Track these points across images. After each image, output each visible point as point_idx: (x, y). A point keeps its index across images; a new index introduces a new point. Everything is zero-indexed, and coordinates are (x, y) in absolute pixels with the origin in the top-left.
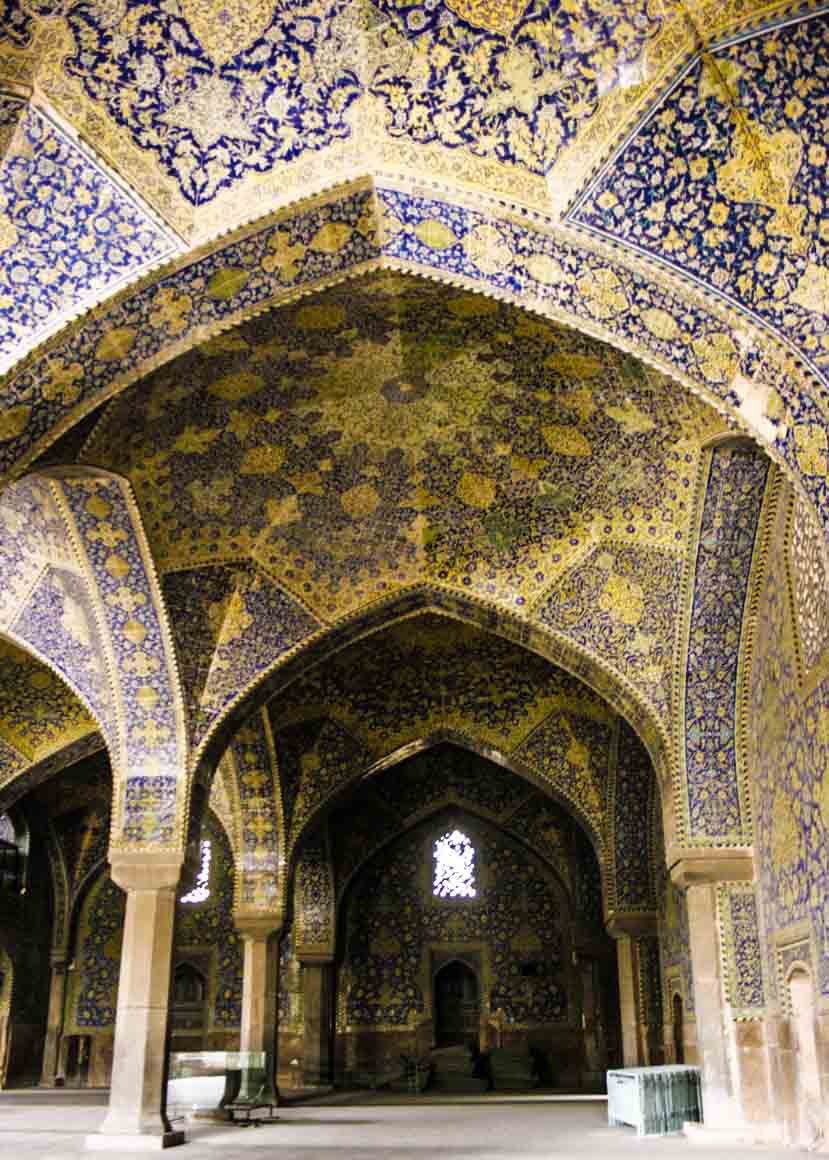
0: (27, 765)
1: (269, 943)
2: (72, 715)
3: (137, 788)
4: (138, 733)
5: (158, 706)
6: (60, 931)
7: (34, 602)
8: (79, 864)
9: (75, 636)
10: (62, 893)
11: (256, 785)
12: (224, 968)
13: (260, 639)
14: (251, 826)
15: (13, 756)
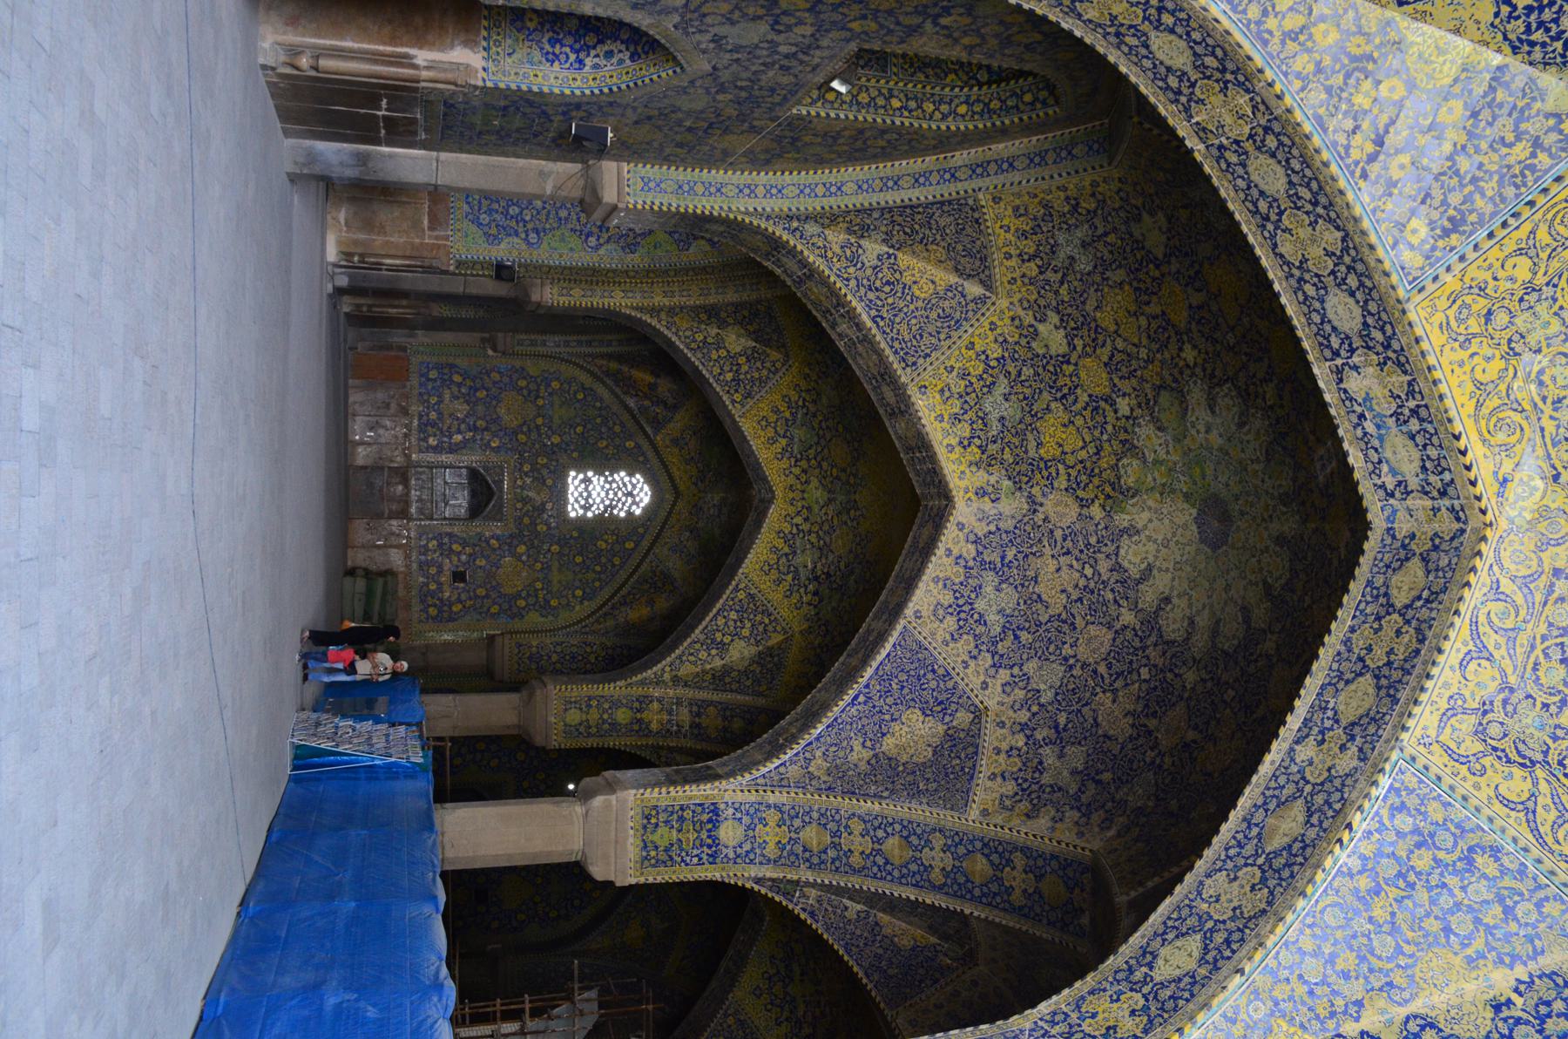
0: (736, 411)
1: (519, 727)
2: (797, 471)
3: (705, 817)
4: (772, 817)
5: (805, 850)
6: (533, 343)
7: (941, 671)
8: (614, 365)
9: (896, 727)
10: (580, 343)
11: (704, 721)
12: (487, 542)
13: (880, 951)
14: (656, 705)
15: (749, 395)
